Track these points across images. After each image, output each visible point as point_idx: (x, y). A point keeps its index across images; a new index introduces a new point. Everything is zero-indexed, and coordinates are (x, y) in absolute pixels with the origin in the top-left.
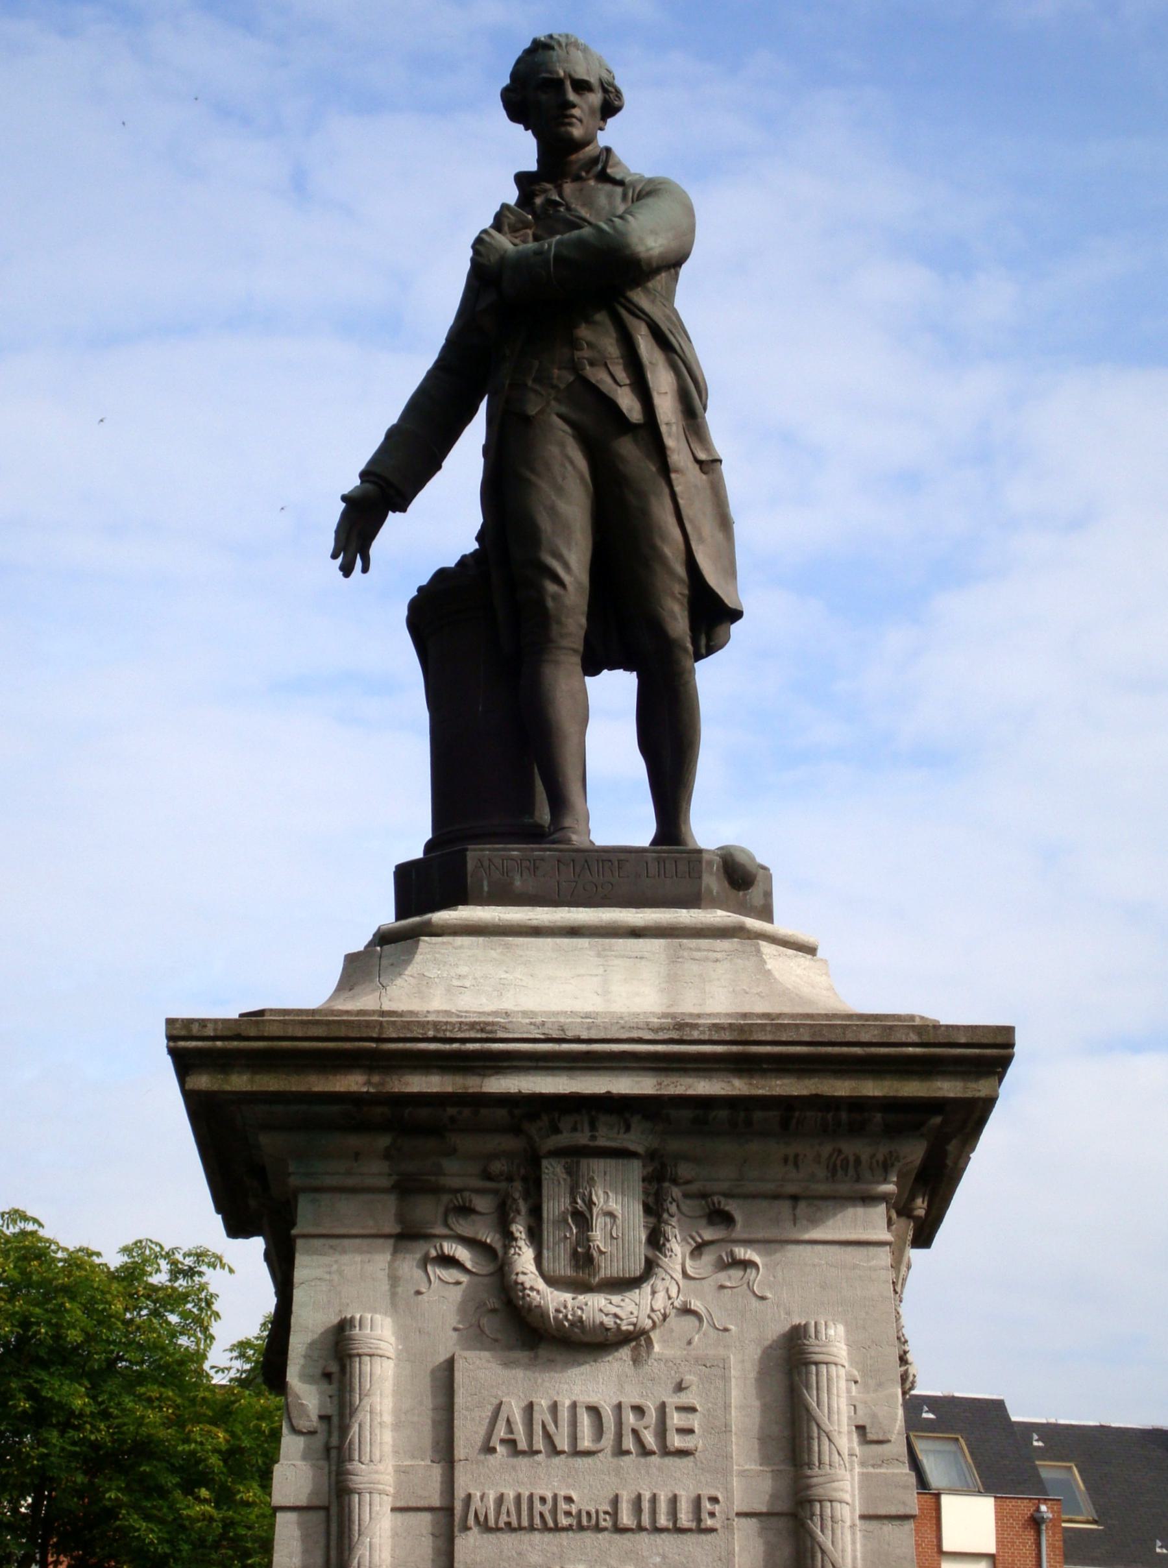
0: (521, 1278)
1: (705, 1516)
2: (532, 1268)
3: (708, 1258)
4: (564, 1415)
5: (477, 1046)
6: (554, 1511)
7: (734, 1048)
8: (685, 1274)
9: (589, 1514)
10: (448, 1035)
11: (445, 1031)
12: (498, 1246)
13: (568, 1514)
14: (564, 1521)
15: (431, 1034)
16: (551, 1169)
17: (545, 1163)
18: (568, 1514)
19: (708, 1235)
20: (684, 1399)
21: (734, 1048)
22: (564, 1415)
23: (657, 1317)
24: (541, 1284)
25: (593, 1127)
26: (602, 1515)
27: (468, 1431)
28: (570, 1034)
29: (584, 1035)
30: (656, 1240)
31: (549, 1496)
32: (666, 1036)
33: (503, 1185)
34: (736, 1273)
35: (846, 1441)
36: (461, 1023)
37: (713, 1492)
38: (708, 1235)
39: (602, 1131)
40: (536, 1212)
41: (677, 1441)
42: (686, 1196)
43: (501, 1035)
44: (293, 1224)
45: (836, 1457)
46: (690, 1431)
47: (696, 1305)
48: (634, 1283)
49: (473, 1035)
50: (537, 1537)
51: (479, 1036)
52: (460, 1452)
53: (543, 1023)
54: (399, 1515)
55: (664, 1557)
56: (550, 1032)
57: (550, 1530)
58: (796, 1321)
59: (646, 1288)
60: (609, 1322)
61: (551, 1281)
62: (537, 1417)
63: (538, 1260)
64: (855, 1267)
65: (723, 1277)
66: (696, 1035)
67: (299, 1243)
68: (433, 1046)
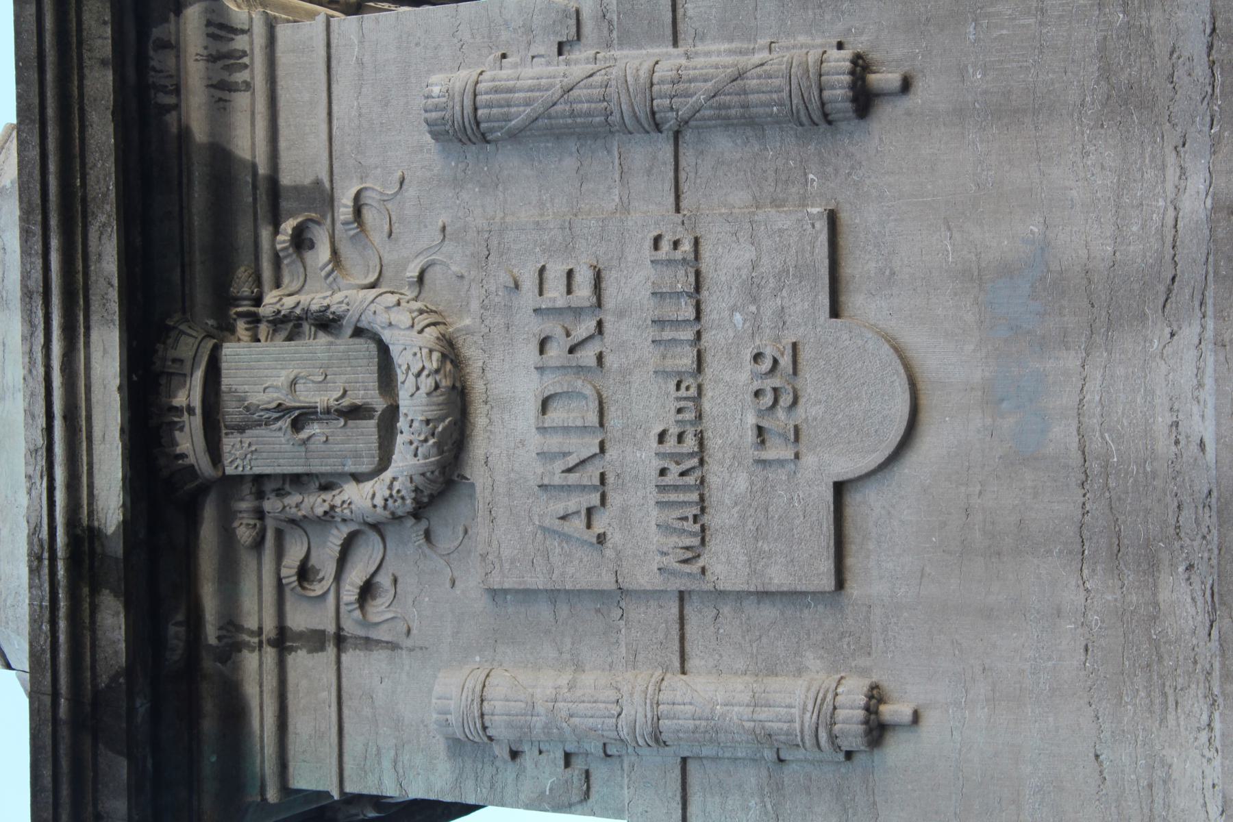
0: (379, 501)
1: (678, 255)
2: (368, 487)
3: (346, 250)
4: (554, 442)
5: (61, 565)
6: (677, 458)
7: (53, 222)
8: (373, 286)
9: (679, 411)
10: (46, 603)
11: (41, 606)
12: (345, 530)
13: (680, 438)
14: (690, 444)
15: (46, 627)
16: (239, 461)
17: (230, 470)
18: (680, 438)
19: (323, 253)
20: (529, 282)
21: (53, 222)
22: (554, 442)
23: (423, 320)
24: (387, 475)
25: (178, 410)
26: (683, 393)
27: (582, 571)
28: (41, 441)
29: (41, 421)
30: (326, 323)
31: (658, 464)
32: (40, 314)
33: (271, 525)
34: (369, 215)
35: (578, 65)
36: (31, 587)
37: (649, 243)
38: (323, 253)
39: (180, 400)
40: (297, 481)
41: (583, 291)
42: (278, 285)
43: (45, 534)
44: (327, 794)
45: (597, 78)
46: (570, 274)
47: (413, 271)
48: (384, 350)
49: (45, 571)
50: (713, 480)
51: (46, 562)
52: (606, 581)
53: (29, 477)
54: (689, 665)
55: (733, 309)
56: (39, 468)
57: (702, 462)
58: (428, 137)
59: (386, 336)
60: (427, 383)
61: (384, 462)
62: (558, 479)
63: (358, 478)
64: (360, 63)
65: (377, 236)
66: (37, 274)
67: (350, 788)
68: (62, 624)
